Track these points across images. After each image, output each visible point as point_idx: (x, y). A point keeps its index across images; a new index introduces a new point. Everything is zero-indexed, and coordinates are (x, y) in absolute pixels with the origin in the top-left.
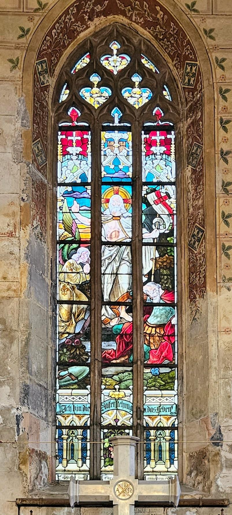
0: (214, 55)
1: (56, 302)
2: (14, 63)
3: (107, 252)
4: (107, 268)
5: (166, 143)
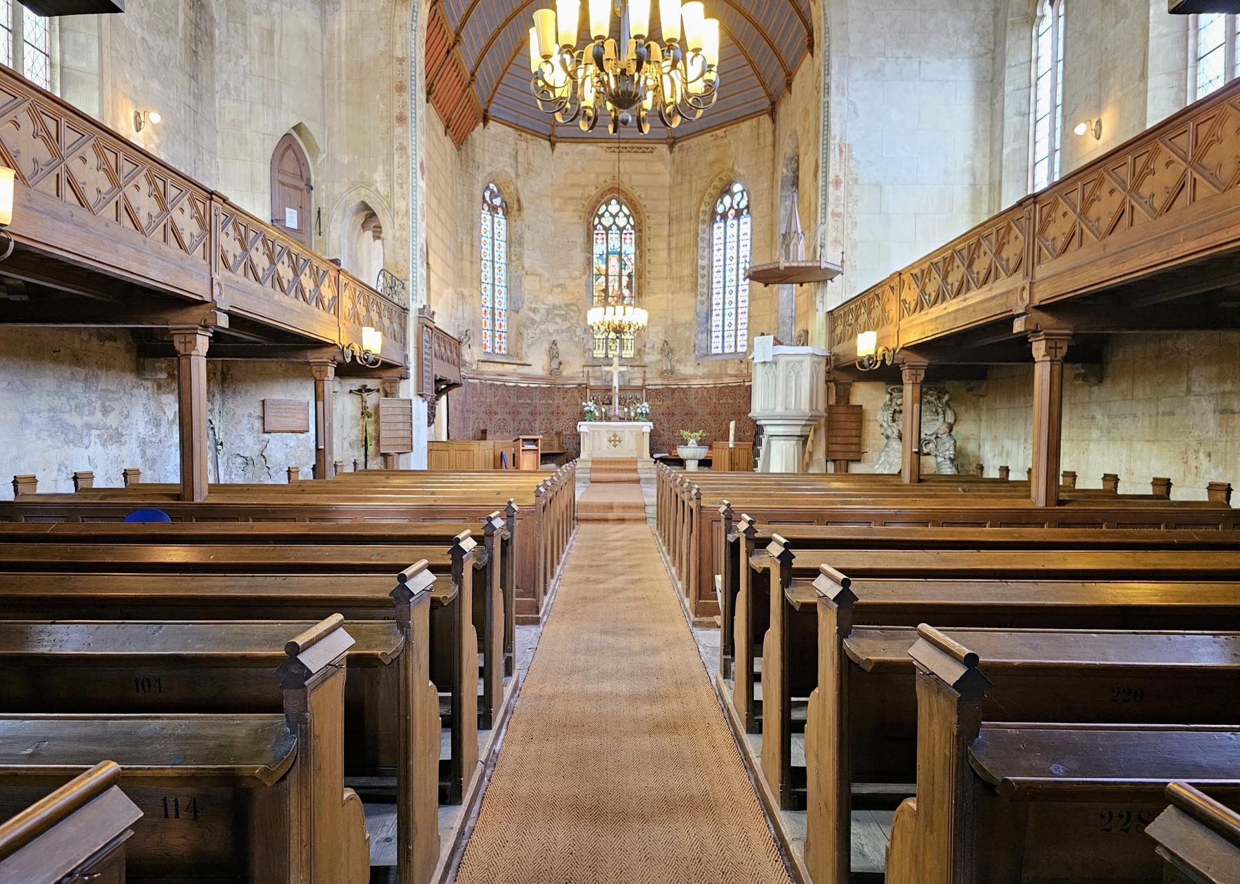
0: (647, 214)
2: (580, 217)
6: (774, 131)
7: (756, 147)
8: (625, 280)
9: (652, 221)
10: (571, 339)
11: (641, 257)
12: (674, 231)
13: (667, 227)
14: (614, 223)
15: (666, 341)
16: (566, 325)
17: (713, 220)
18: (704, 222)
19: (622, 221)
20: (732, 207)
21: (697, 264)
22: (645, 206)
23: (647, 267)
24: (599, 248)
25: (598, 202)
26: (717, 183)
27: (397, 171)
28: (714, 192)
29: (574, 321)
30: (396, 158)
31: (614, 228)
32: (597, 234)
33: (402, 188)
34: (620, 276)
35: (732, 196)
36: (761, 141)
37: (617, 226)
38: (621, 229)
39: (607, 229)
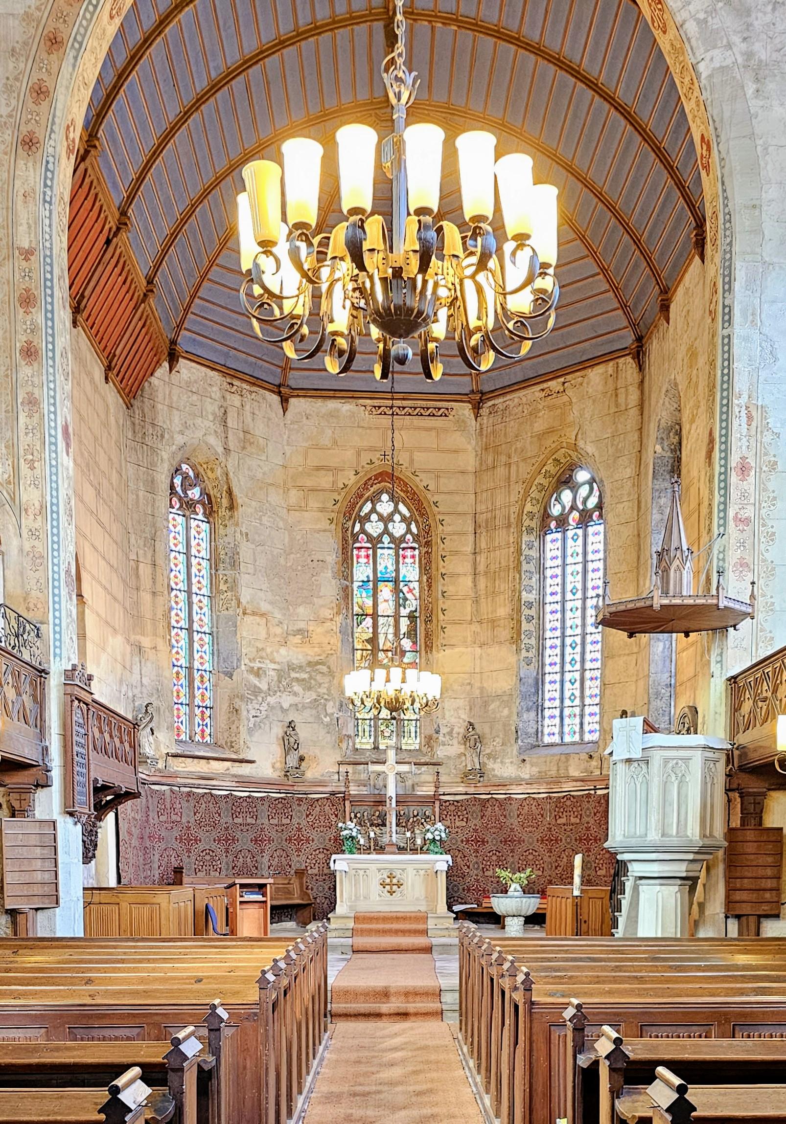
0: (438, 517)
1: (354, 650)
3: (381, 620)
4: (381, 630)
5: (413, 557)
6: (642, 382)
7: (612, 411)
8: (404, 623)
9: (448, 529)
10: (318, 717)
11: (430, 587)
12: (483, 545)
13: (471, 538)
14: (386, 531)
15: (471, 724)
16: (310, 696)
17: (544, 529)
18: (530, 530)
19: (398, 529)
20: (573, 508)
21: (520, 600)
22: (435, 503)
23: (440, 602)
24: (362, 571)
25: (361, 496)
26: (550, 467)
27: (24, 441)
28: (545, 482)
29: (323, 690)
30: (22, 418)
31: (386, 539)
32: (359, 548)
33: (32, 468)
34: (397, 617)
35: (574, 489)
36: (622, 399)
37: (391, 535)
38: (397, 542)
39: (375, 542)
